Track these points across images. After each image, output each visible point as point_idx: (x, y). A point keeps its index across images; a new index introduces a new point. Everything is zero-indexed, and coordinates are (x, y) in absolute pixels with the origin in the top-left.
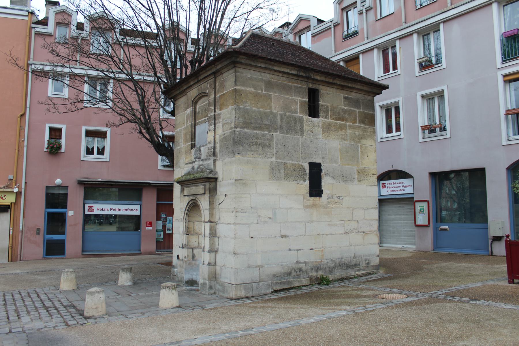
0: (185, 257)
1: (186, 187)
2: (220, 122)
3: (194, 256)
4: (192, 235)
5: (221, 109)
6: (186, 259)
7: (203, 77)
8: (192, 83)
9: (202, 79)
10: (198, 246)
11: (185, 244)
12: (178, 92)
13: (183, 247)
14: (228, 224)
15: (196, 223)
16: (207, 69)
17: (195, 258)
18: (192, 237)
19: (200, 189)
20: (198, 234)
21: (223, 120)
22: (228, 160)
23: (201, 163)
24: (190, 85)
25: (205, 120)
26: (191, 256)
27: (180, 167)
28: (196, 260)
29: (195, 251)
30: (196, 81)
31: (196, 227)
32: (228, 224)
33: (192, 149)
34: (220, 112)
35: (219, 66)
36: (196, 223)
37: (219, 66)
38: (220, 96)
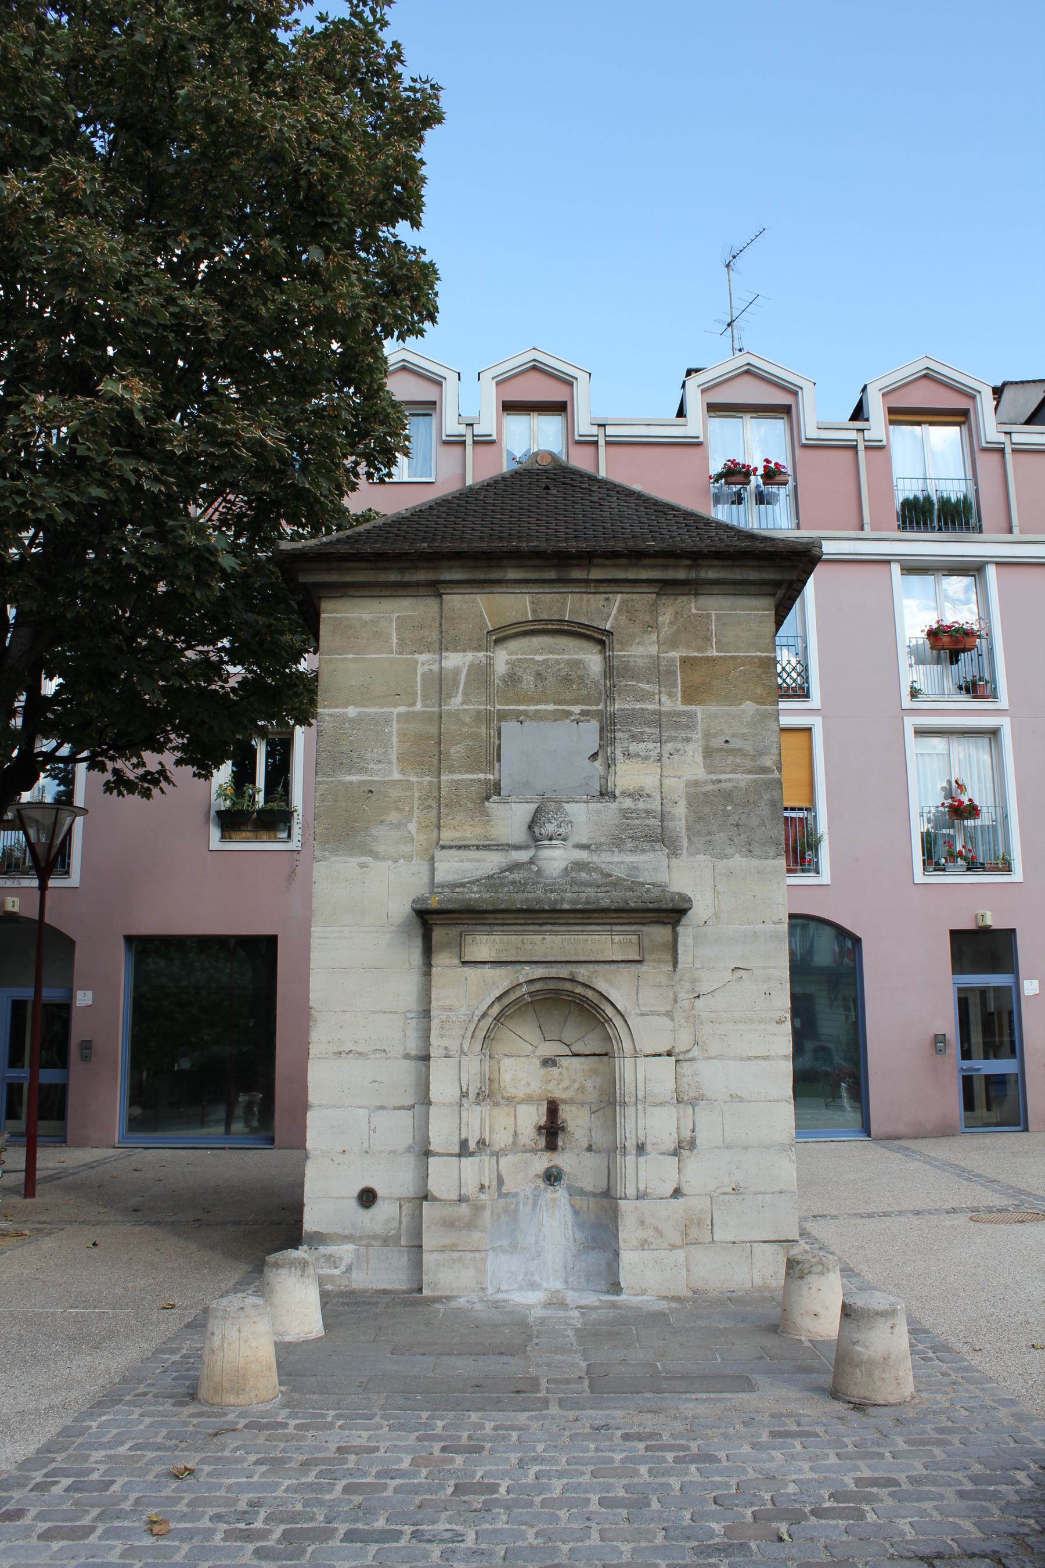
0: (482, 1187)
1: (490, 933)
2: (688, 740)
3: (500, 1181)
4: (496, 1104)
5: (688, 699)
6: (483, 1197)
7: (596, 574)
8: (512, 574)
9: (587, 581)
10: (514, 1143)
11: (481, 1142)
12: (393, 577)
13: (464, 1150)
14: (749, 1058)
15: (507, 1063)
16: (646, 562)
17: (504, 1191)
18: (496, 1111)
19: (604, 943)
20: (511, 1101)
21: (707, 735)
22: (738, 861)
23: (582, 855)
24: (495, 575)
25: (568, 714)
26: (495, 1183)
27: (371, 853)
28: (506, 1195)
29: (503, 1161)
30: (553, 575)
31: (506, 1077)
32: (749, 1058)
33: (488, 798)
34: (680, 707)
35: (711, 574)
36: (507, 1063)
37: (711, 574)
38: (684, 661)
